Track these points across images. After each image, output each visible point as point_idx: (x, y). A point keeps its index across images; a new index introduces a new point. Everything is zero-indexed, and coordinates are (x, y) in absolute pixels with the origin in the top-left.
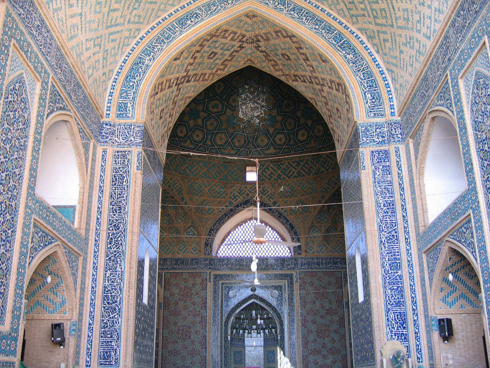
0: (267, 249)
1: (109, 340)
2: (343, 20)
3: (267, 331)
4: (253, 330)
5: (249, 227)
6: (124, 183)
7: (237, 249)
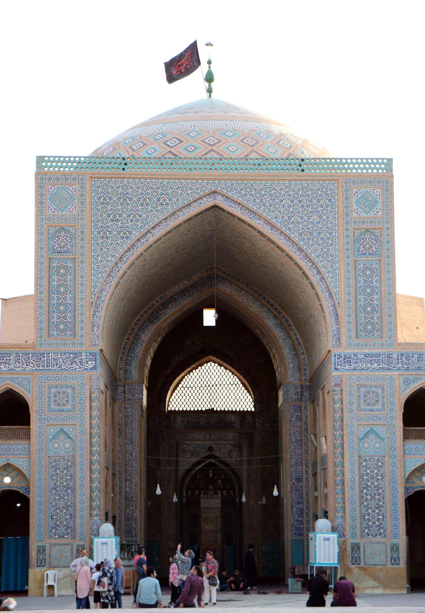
0: (226, 397)
1: (131, 522)
2: (277, 307)
3: (225, 492)
4: (210, 490)
5: (205, 371)
6: (134, 426)
7: (192, 397)
